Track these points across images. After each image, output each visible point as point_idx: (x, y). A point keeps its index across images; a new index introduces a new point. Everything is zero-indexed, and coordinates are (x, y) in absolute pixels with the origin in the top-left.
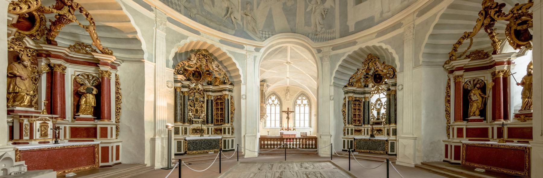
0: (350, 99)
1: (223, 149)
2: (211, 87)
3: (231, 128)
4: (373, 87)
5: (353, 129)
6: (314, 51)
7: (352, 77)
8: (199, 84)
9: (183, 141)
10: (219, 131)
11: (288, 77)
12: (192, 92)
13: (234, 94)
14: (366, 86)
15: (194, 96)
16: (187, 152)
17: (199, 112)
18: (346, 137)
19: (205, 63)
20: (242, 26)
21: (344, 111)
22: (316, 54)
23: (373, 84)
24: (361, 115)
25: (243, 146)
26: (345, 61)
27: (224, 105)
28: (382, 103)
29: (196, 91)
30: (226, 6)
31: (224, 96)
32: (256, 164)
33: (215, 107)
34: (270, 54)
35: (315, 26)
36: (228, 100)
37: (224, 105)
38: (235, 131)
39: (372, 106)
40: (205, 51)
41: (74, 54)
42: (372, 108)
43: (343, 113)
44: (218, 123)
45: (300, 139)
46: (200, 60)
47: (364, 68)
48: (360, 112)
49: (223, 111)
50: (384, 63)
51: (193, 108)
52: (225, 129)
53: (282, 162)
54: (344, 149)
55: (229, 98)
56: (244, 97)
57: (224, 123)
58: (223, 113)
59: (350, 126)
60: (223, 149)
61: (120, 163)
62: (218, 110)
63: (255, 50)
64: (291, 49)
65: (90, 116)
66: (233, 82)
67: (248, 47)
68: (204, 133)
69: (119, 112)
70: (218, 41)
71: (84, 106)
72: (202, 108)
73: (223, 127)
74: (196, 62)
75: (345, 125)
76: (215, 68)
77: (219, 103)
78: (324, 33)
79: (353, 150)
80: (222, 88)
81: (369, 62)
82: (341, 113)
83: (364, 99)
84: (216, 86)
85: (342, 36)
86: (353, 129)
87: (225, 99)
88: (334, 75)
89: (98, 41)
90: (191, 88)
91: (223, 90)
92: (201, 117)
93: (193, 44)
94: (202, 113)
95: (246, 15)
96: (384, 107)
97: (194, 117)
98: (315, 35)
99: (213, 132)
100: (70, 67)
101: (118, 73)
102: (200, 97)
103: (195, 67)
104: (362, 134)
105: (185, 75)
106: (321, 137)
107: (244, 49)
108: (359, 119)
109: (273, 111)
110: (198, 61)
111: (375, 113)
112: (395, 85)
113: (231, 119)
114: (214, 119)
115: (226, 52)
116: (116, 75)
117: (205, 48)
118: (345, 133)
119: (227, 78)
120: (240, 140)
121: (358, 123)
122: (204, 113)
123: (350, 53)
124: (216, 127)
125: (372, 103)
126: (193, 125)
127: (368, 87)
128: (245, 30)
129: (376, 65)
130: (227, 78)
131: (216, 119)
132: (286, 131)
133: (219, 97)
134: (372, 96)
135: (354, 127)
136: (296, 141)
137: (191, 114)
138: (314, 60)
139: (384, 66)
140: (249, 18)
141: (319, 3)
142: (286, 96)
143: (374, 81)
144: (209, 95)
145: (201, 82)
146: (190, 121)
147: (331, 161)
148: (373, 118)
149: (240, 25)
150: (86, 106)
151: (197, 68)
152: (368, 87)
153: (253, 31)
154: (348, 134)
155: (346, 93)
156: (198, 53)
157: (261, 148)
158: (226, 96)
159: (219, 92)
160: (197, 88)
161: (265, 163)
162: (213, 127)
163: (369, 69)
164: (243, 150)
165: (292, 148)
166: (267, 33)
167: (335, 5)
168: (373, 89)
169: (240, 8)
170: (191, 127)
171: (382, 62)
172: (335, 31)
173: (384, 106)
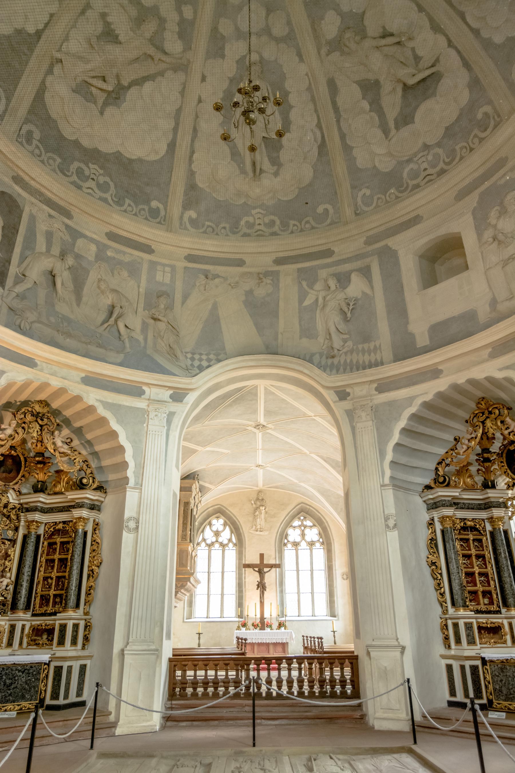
0: (448, 524)
1: (48, 701)
2: (42, 498)
3: (82, 624)
6: (330, 396)
7: (443, 460)
8: (11, 491)
10: (45, 637)
11: (260, 463)
18: (453, 652)
19: (35, 435)
20: (143, 344)
21: (434, 564)
22: (334, 402)
23: (508, 479)
24: (490, 576)
26: (414, 417)
27: (71, 552)
30: (109, 302)
31: (75, 523)
32: (154, 761)
34: (211, 407)
35: (328, 337)
36: (85, 534)
37: (71, 552)
38: (95, 635)
40: (42, 403)
43: (433, 570)
44: (45, 608)
45: (300, 660)
46: (23, 428)
48: (485, 564)
49: (66, 567)
52: (63, 628)
53: (241, 753)
54: (453, 699)
55: (89, 528)
56: (132, 525)
57: (65, 609)
58: (67, 574)
60: (48, 701)
62: (53, 568)
63: (171, 397)
64: (267, 392)
66: (107, 482)
67: (154, 390)
70: (79, 380)
73: (57, 621)
74: (13, 433)
75: (445, 611)
76: (62, 447)
77: (59, 544)
78: (352, 351)
79: (484, 701)
80: (73, 500)
82: (427, 571)
83: (491, 522)
84: (56, 493)
85: (398, 358)
86: (471, 623)
87: (76, 532)
88: (389, 456)
91: (73, 507)
93: (14, 389)
95: (155, 319)
98: (327, 358)
99: (25, 640)
102: (7, 528)
103: (8, 446)
104: (505, 642)
106: (368, 653)
107: (143, 396)
108: (487, 589)
110: (20, 430)
113: (88, 594)
114: (36, 593)
115: (96, 404)
117: (42, 397)
118: (446, 638)
120: (106, 669)
122: (8, 575)
123: (428, 397)
124: (38, 623)
127: (493, 487)
128: (149, 352)
130: (89, 471)
131: (42, 596)
132: (257, 631)
133: (60, 526)
135: (476, 618)
136: (290, 670)
138: (330, 418)
140: (162, 326)
141: (333, 287)
142: (255, 517)
143: (509, 471)
144: (33, 521)
145: (16, 483)
147: (414, 747)
149: (137, 341)
151: (12, 447)
152: (493, 487)
154: (458, 641)
155: (433, 506)
156: (23, 410)
157: (172, 695)
158: (81, 523)
159: (62, 511)
161: (183, 756)
162: (28, 621)
163: (490, 439)
164: (112, 706)
165: (274, 694)
166: (204, 357)
167: (373, 291)
168: (510, 492)
169: (141, 305)
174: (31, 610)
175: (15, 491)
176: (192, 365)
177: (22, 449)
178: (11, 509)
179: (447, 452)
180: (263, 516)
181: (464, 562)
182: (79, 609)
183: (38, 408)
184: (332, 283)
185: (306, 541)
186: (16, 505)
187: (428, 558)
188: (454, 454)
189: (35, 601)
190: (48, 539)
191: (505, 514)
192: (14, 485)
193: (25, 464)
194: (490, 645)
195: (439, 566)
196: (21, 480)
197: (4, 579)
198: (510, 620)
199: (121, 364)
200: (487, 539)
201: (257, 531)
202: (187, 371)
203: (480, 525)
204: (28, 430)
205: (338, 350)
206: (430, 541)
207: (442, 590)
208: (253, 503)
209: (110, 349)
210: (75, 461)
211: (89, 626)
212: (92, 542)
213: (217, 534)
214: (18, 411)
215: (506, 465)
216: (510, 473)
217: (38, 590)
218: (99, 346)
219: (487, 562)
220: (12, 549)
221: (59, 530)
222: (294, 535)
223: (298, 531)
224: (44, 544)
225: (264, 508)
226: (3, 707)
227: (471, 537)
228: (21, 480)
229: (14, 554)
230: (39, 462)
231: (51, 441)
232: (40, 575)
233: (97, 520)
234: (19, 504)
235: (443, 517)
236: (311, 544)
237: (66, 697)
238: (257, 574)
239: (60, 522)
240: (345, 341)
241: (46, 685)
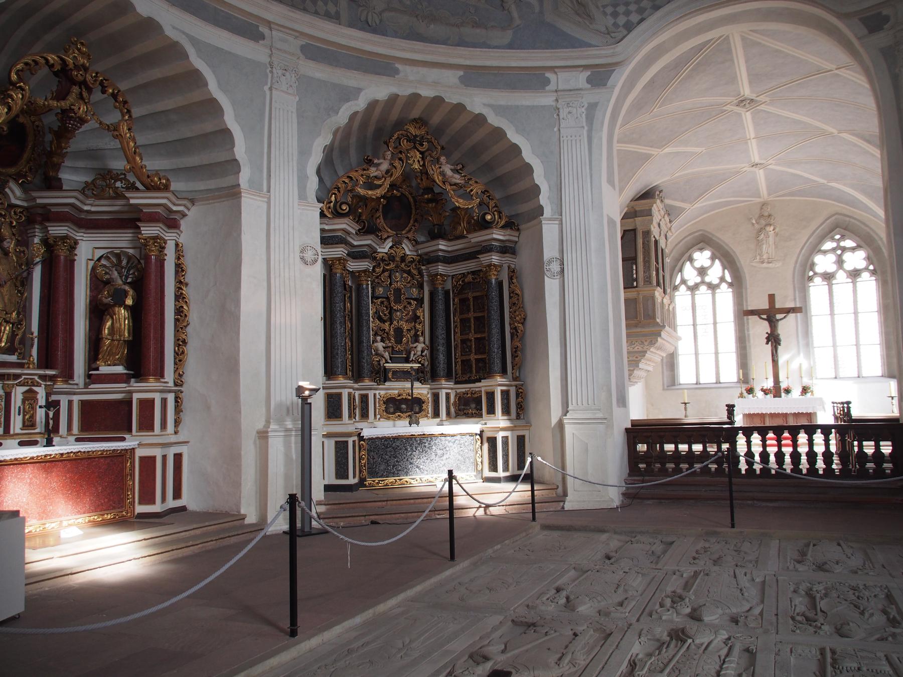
2: (443, 245)
8: (405, 241)
9: (354, 442)
10: (473, 406)
12: (384, 271)
13: (523, 261)
15: (391, 284)
20: (537, 10)
29: (397, 267)
33: (458, 314)
36: (500, 284)
41: (92, 205)
46: (400, 159)
61: (183, 509)
63: (589, 80)
65: (120, 369)
66: (517, 215)
67: (563, 75)
68: (423, 413)
69: (183, 353)
70: (457, 81)
71: (108, 342)
72: (416, 322)
76: (452, 177)
87: (488, 282)
89: (138, 159)
92: (412, 355)
94: (417, 341)
97: (391, 358)
99: (452, 410)
100: (84, 239)
101: (181, 240)
103: (387, 185)
105: (360, 215)
107: (547, 88)
110: (397, 163)
113: (514, 356)
115: (485, 111)
116: (177, 245)
117: (415, 113)
119: (492, 204)
122: (421, 339)
124: (464, 390)
126: (387, 384)
130: (492, 204)
131: (462, 361)
133: (469, 278)
137: (380, 345)
144: (437, 275)
150: (113, 340)
151: (393, 186)
153: (578, 14)
156: (396, 136)
166: (633, 7)
170: (383, 392)
175: (410, 240)
176: (615, 25)
177: (408, 187)
178: (409, 262)
180: (771, 240)
182: (507, 374)
183: (413, 131)
185: (845, 271)
189: (456, 367)
190: (459, 294)
193: (415, 205)
197: (417, 344)
199: (510, 46)
201: (763, 262)
202: (609, 36)
204: (407, 162)
208: (754, 221)
209: (492, 26)
210: (472, 193)
211: (522, 393)
212: (510, 294)
213: (702, 271)
214: (391, 138)
218: (476, 25)
220: (421, 310)
222: (824, 263)
223: (832, 257)
225: (772, 228)
229: (424, 315)
230: (429, 201)
232: (456, 338)
233: (513, 266)
234: (417, 256)
236: (855, 274)
238: (766, 323)
239: (468, 273)
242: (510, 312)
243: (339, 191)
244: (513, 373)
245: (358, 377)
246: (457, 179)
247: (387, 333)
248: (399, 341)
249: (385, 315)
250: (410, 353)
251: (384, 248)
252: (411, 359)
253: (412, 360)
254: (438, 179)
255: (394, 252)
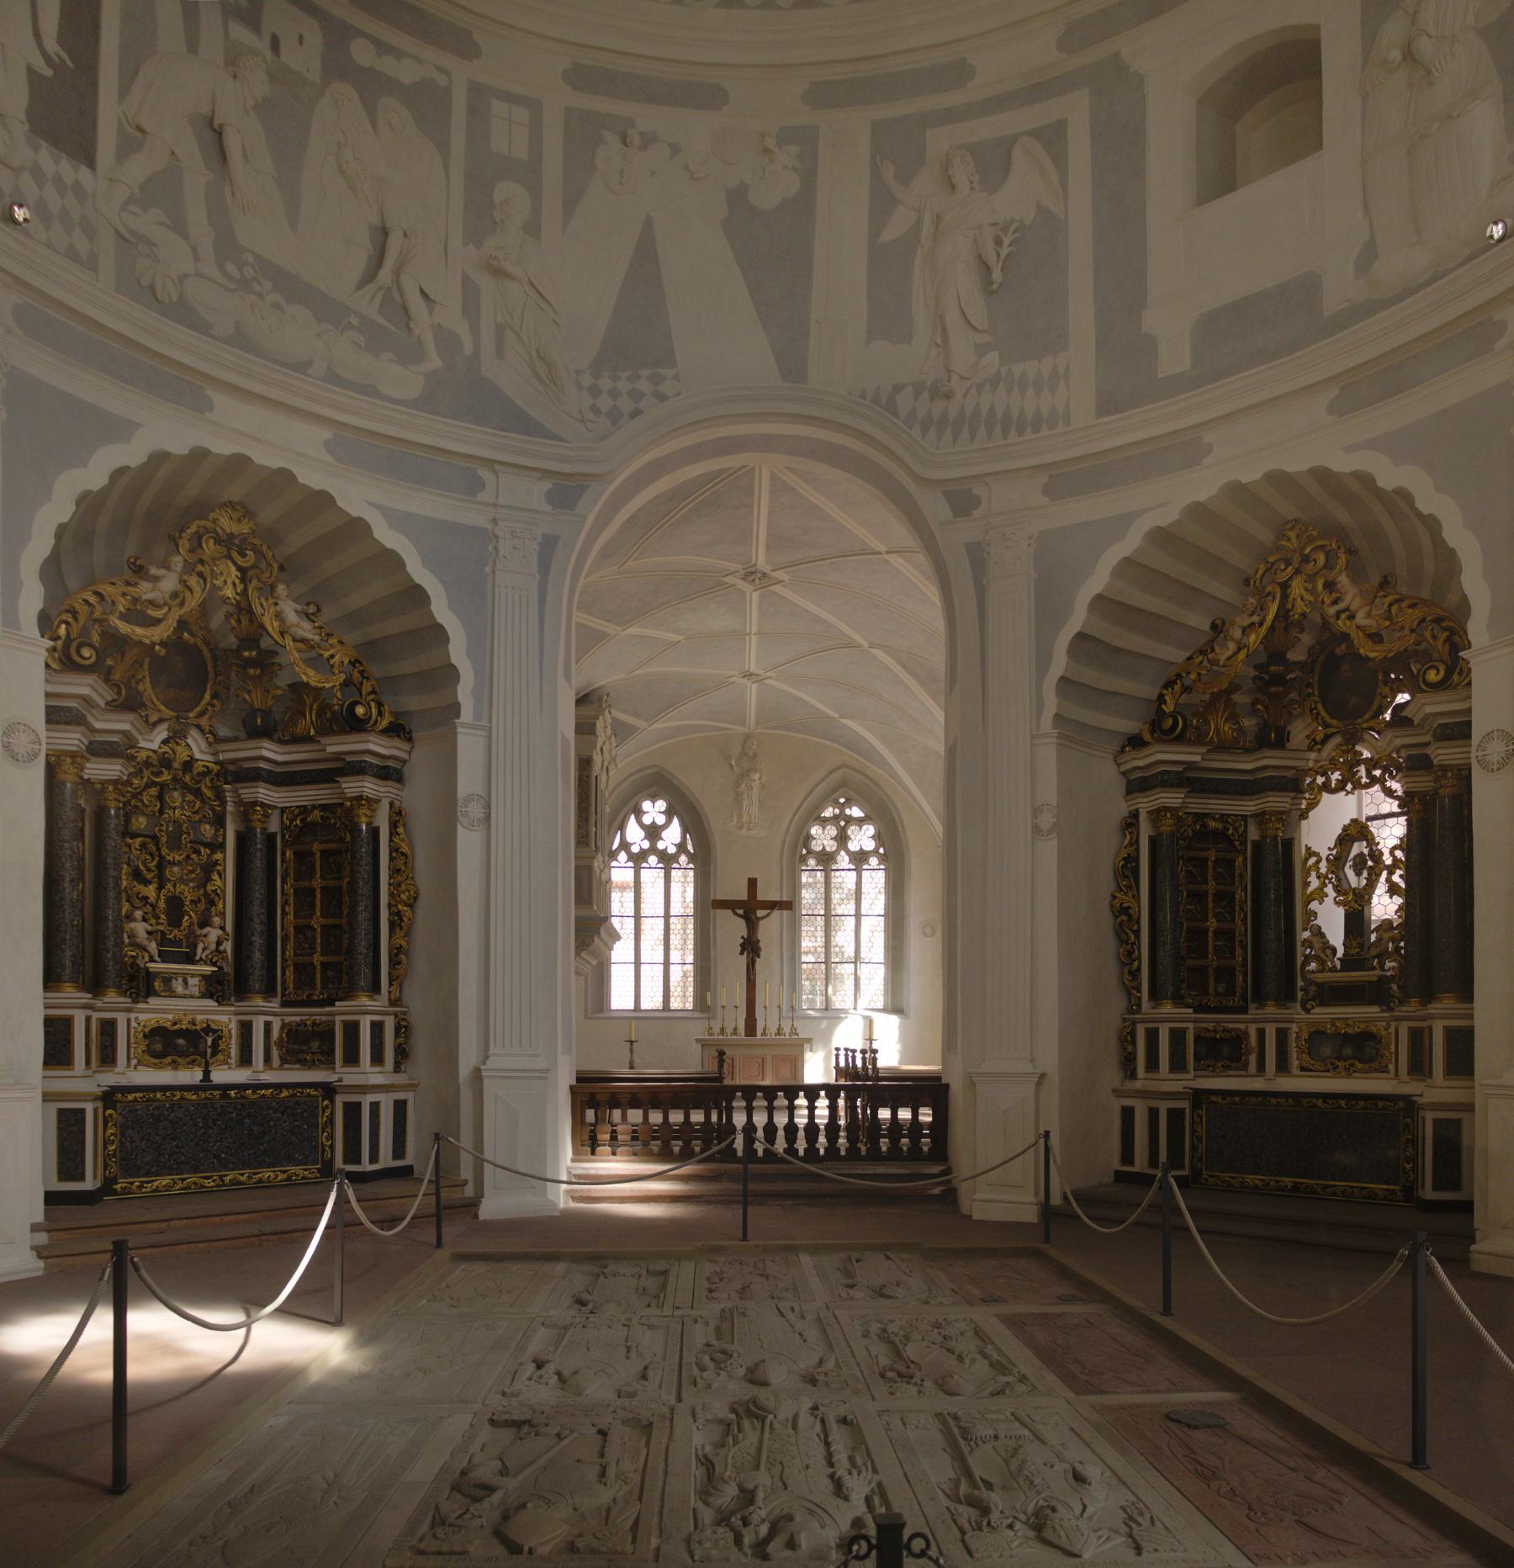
0: (1166, 828)
1: (339, 1163)
2: (270, 751)
3: (389, 1024)
4: (1315, 744)
5: (1184, 1030)
7: (1179, 676)
8: (194, 733)
10: (315, 1045)
12: (147, 786)
13: (417, 796)
14: (1273, 737)
15: (161, 812)
16: (114, 1181)
17: (190, 918)
18: (1138, 1085)
19: (229, 592)
20: (468, 349)
21: (1124, 910)
24: (1238, 938)
25: (466, 1139)
27: (347, 872)
28: (1381, 854)
29: (175, 779)
31: (351, 808)
35: (939, 341)
36: (375, 832)
37: (347, 872)
38: (420, 1044)
39: (1314, 874)
40: (234, 509)
42: (1310, 889)
45: (832, 1091)
46: (201, 575)
47: (1255, 619)
50: (1385, 583)
51: (150, 891)
52: (352, 1030)
55: (383, 822)
57: (349, 994)
59: (1168, 1009)
63: (550, 497)
68: (220, 1057)
74: (180, 587)
75: (1134, 1006)
79: (1185, 1172)
80: (338, 757)
81: (1291, 579)
82: (1107, 922)
83: (1260, 824)
87: (354, 829)
88: (1059, 664)
90: (142, 755)
92: (199, 951)
96: (1388, 880)
97: (160, 953)
98: (932, 398)
99: (275, 1053)
102: (197, 818)
103: (172, 622)
104: (1245, 1067)
105: (110, 670)
109: (653, 901)
110: (194, 581)
111: (1331, 920)
112: (1459, 730)
113: (394, 962)
114: (284, 960)
117: (235, 492)
120: (450, 1109)
121: (1221, 987)
122: (217, 920)
123: (1167, 517)
124: (298, 1019)
125: (1310, 853)
126: (154, 1002)
129: (1334, 595)
131: (296, 966)
133: (316, 815)
134: (1313, 805)
135: (1195, 1021)
137: (140, 928)
139: (1390, 605)
143: (1320, 706)
144: (255, 803)
145: (202, 714)
146: (132, 978)
148: (1317, 958)
151: (182, 624)
154: (1152, 1064)
155: (1137, 785)
156: (193, 529)
158: (363, 811)
160: (182, 755)
162: (275, 1014)
164: (466, 1173)
168: (1313, 755)
170: (143, 1017)
171: (1376, 579)
172: (1067, 370)
173: (1391, 873)
174: (279, 995)
178: (199, 774)
179: (1190, 658)
181: (1188, 907)
182: (380, 993)
184: (962, 173)
186: (211, 765)
187: (1114, 897)
188: (1206, 663)
191: (1292, 805)
192: (197, 717)
193: (215, 666)
194: (1212, 1071)
195: (1135, 916)
196: (213, 706)
198: (1261, 1025)
200: (1245, 859)
203: (1236, 829)
205: (962, 377)
206: (1123, 862)
207: (1136, 963)
211: (406, 1027)
214: (182, 530)
215: (1316, 693)
216: (1323, 713)
217: (287, 953)
219: (1237, 908)
221: (314, 824)
224: (284, 857)
226: (255, 1174)
227: (1212, 855)
228: (213, 706)
231: (272, 610)
232: (286, 919)
233: (397, 804)
234: (215, 763)
235: (1158, 811)
237: (374, 1158)
239: (314, 807)
240: (981, 350)
241: (332, 1138)
242: (390, 885)
243: (75, 618)
244: (390, 992)
245: (96, 986)
246: (306, 630)
247: (151, 905)
248: (175, 922)
249: (149, 870)
250: (195, 947)
251: (152, 741)
252: (198, 958)
253: (201, 959)
254: (272, 626)
255: (170, 752)
